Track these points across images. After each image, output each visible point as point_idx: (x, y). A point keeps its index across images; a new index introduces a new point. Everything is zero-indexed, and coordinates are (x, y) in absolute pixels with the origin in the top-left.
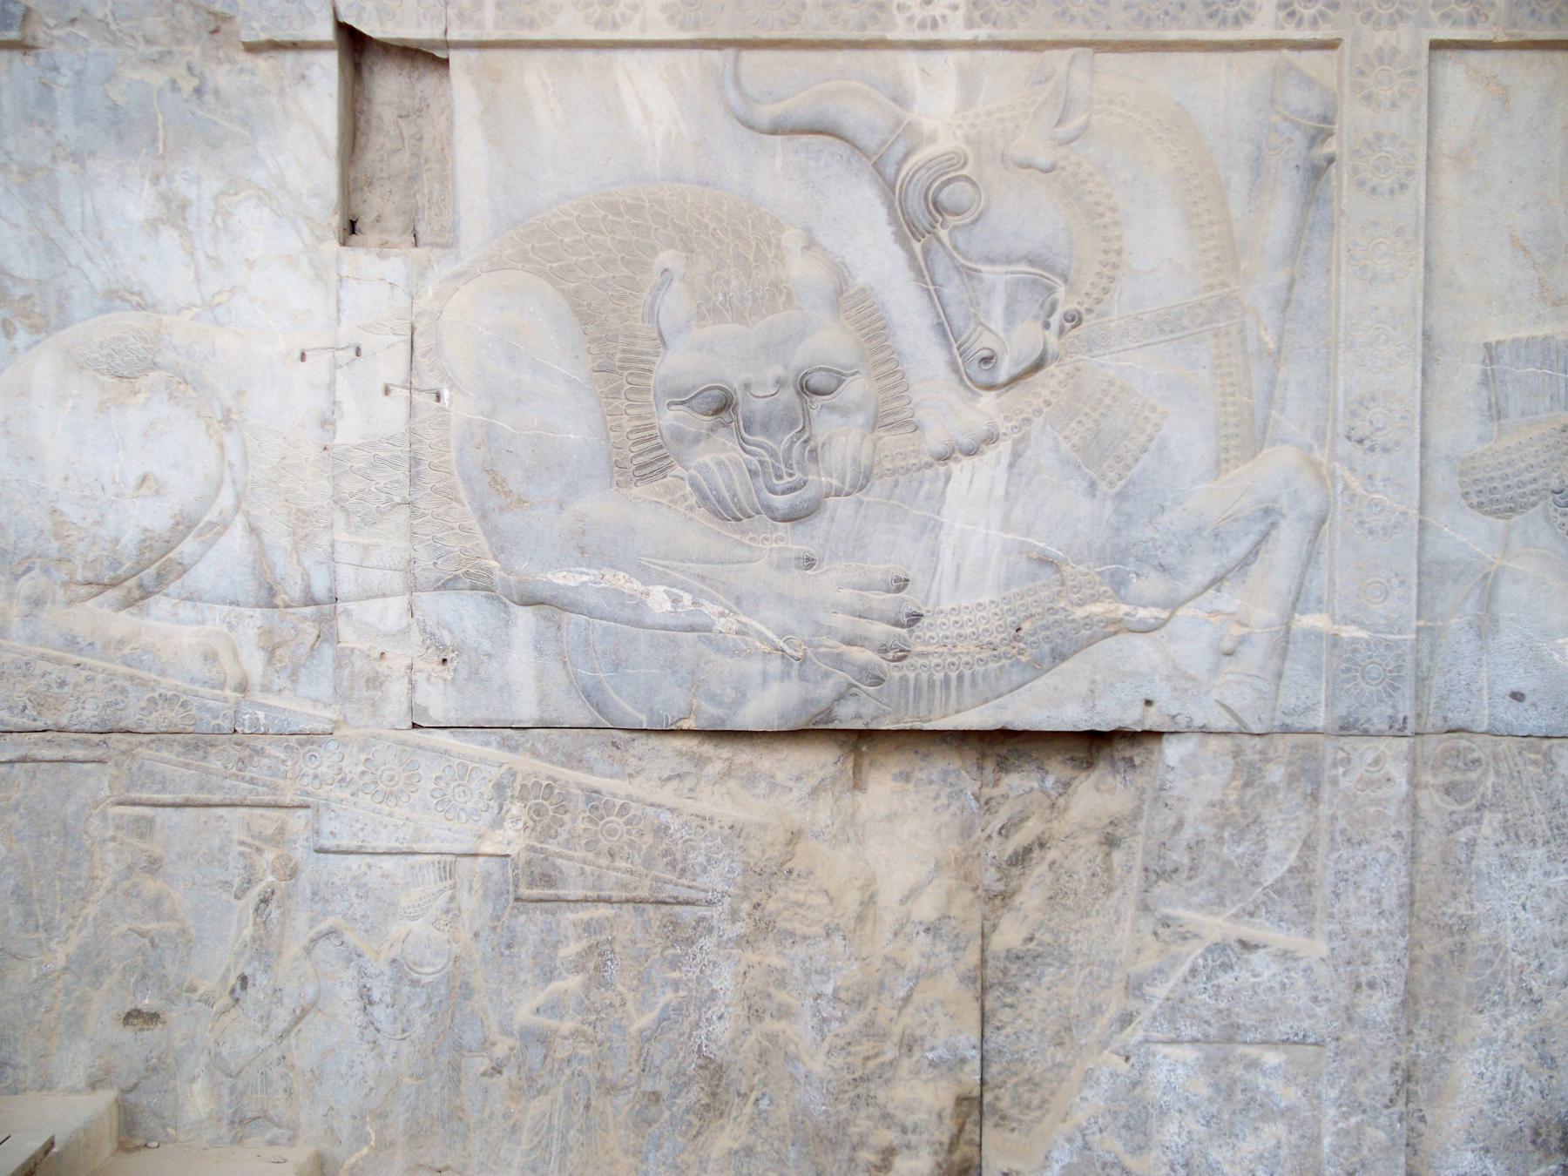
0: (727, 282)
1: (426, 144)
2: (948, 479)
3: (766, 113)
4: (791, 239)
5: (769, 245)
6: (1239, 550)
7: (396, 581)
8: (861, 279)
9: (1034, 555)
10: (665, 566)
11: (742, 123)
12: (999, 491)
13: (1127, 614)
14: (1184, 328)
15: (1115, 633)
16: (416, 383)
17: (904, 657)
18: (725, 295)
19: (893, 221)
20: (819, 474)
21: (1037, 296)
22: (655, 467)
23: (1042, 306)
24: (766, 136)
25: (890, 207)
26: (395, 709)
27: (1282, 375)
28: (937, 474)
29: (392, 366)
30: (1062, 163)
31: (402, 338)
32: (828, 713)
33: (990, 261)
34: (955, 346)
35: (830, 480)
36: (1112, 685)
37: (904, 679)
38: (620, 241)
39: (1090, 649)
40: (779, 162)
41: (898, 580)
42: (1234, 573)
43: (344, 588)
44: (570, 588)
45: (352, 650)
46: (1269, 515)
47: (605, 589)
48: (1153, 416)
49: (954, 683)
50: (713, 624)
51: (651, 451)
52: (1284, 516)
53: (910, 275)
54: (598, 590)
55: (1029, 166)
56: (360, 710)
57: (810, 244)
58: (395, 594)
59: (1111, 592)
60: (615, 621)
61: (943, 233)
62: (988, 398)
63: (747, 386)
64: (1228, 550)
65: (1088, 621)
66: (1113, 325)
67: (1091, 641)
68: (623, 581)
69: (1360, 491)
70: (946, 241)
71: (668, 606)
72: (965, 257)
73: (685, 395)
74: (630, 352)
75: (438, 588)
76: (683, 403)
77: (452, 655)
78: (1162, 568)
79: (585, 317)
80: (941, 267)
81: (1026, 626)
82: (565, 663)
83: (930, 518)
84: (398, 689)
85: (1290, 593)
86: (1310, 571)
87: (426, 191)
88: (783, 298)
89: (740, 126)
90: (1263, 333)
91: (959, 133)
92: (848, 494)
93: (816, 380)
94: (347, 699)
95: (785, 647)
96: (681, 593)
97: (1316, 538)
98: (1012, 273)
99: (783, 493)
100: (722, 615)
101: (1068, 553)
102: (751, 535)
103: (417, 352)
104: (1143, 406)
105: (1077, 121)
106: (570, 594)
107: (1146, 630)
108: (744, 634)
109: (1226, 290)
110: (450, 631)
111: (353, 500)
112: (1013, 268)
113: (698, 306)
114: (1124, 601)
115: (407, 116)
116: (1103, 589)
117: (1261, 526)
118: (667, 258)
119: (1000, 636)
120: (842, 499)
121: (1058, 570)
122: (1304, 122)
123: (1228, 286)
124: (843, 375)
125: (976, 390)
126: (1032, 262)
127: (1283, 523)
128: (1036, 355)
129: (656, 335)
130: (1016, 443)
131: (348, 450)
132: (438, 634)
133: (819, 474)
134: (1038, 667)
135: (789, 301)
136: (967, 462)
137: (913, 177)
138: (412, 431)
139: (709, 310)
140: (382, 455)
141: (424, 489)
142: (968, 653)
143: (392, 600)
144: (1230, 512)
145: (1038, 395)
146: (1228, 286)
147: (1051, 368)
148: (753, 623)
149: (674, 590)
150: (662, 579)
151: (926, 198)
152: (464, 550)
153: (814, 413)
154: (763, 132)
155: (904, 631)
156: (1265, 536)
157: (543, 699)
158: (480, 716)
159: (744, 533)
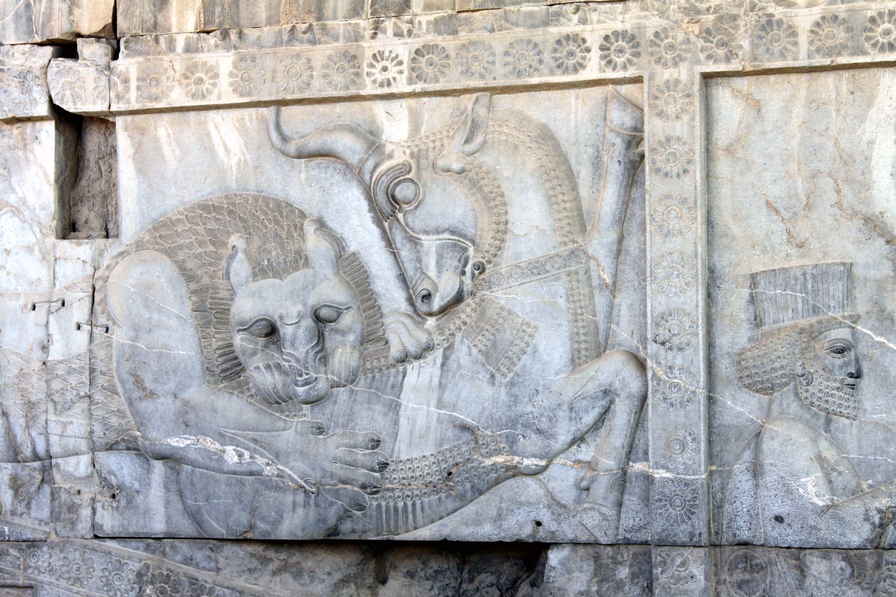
0: (270, 252)
2: (405, 374)
5: (295, 229)
6: (589, 418)
7: (83, 445)
8: (352, 247)
9: (457, 423)
12: (436, 381)
13: (518, 463)
14: (547, 272)
15: (514, 476)
16: (94, 323)
18: (268, 260)
21: (456, 254)
22: (233, 371)
23: (459, 260)
24: (295, 160)
26: (83, 527)
27: (617, 301)
28: (398, 372)
29: (79, 312)
30: (468, 167)
32: (335, 531)
33: (427, 232)
36: (512, 511)
37: (379, 506)
39: (497, 487)
40: (303, 176)
41: (373, 440)
42: (589, 434)
43: (55, 449)
44: (181, 449)
45: (60, 488)
48: (529, 330)
49: (410, 508)
50: (263, 470)
52: (618, 395)
53: (383, 244)
54: (196, 449)
55: (448, 171)
56: (64, 527)
58: (83, 453)
59: (507, 448)
60: (207, 469)
61: (400, 216)
62: (431, 322)
64: (581, 419)
65: (494, 467)
66: (503, 271)
67: (497, 482)
69: (664, 377)
70: (402, 220)
71: (236, 459)
72: (413, 231)
73: (246, 325)
75: (107, 450)
76: (245, 330)
78: (539, 432)
79: (188, 276)
80: (398, 238)
83: (394, 401)
84: (86, 512)
85: (623, 447)
86: (639, 432)
88: (303, 262)
91: (408, 151)
92: (344, 386)
94: (58, 519)
96: (243, 451)
97: (641, 409)
99: (302, 386)
100: (268, 464)
103: (96, 302)
105: (479, 139)
106: (181, 452)
107: (534, 473)
108: (282, 477)
109: (575, 245)
110: (115, 476)
111: (58, 395)
112: (441, 236)
114: (514, 453)
115: (103, 158)
116: (502, 446)
118: (236, 240)
120: (341, 389)
121: (473, 433)
122: (622, 131)
126: (453, 232)
130: (446, 349)
131: (56, 364)
132: (108, 478)
133: (326, 373)
134: (463, 500)
135: (307, 263)
136: (416, 364)
138: (90, 351)
140: (74, 366)
141: (97, 387)
142: (418, 489)
143: (81, 456)
147: (469, 301)
149: (239, 449)
150: (233, 441)
151: (387, 194)
153: (327, 334)
154: (293, 157)
155: (377, 475)
156: (607, 410)
157: (169, 518)
158: (133, 529)
159: (282, 412)
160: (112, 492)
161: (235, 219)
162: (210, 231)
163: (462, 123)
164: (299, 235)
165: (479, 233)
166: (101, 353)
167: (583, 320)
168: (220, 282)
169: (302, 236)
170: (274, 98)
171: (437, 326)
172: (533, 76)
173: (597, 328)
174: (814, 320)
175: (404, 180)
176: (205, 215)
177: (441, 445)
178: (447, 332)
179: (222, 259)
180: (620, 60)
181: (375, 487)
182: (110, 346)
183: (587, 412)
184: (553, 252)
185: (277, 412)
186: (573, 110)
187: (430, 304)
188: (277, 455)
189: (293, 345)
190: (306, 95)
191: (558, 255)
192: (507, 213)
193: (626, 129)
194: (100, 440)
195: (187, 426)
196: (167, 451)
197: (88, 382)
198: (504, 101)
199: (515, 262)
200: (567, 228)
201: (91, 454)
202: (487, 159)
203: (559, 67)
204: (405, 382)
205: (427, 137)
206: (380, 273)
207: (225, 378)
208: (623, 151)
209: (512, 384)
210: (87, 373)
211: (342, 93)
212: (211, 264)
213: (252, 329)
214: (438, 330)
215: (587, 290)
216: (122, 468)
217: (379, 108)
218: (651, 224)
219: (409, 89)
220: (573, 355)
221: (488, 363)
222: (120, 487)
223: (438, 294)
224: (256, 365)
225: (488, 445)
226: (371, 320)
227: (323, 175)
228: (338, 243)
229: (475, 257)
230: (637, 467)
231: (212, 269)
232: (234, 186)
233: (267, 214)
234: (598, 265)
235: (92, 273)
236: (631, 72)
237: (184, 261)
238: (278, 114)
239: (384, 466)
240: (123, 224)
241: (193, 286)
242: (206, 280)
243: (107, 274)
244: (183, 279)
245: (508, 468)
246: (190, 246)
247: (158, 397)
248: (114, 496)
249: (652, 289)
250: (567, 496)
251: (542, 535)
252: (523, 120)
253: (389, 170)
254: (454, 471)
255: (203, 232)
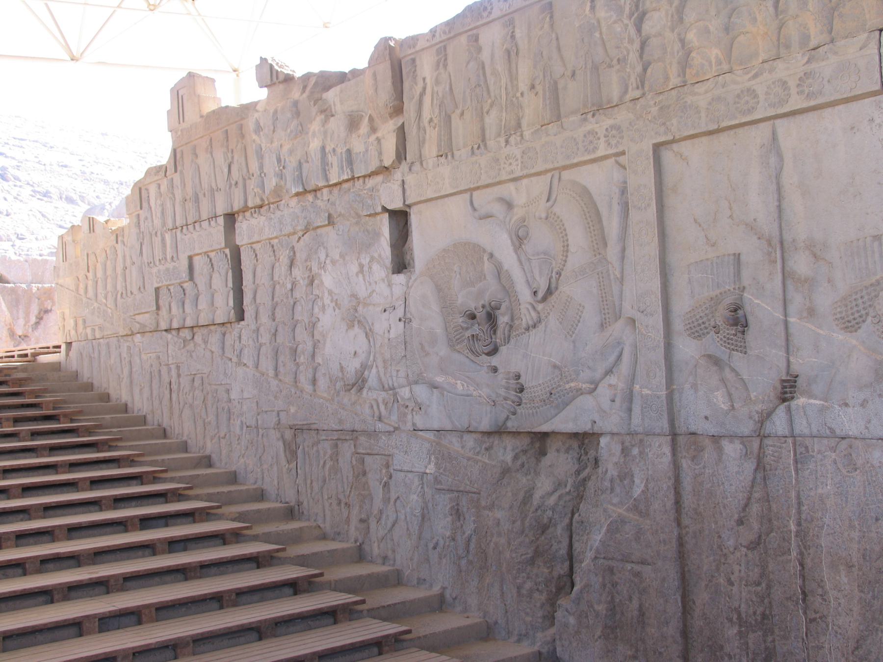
43: (395, 384)
78: (589, 368)
173: (614, 305)
174: (718, 292)
180: (613, 142)
188: (478, 385)
203: (586, 150)
238: (471, 196)
251: (596, 429)
254: (553, 392)
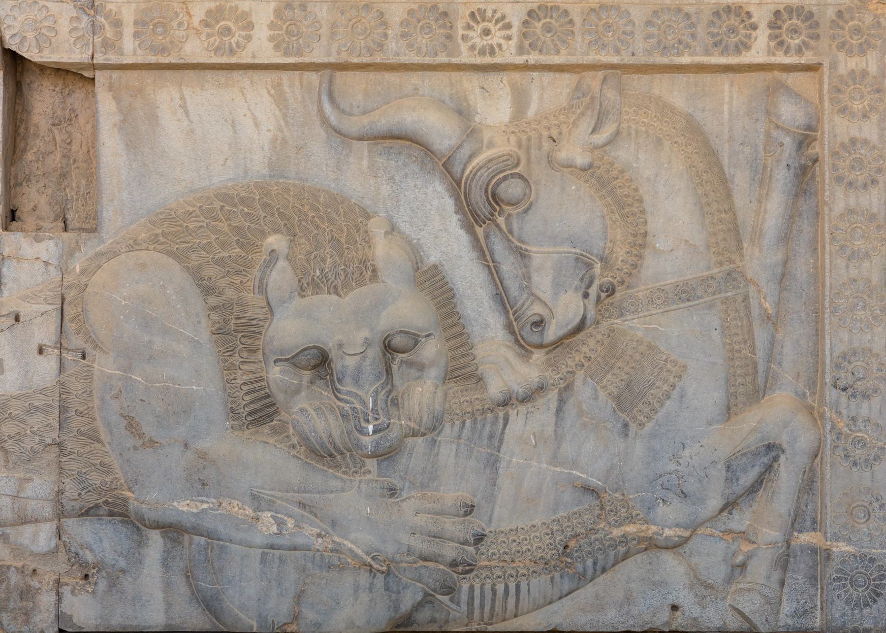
0: (324, 260)
1: (74, 148)
3: (355, 124)
4: (377, 228)
5: (358, 230)
6: (747, 479)
10: (272, 496)
11: (336, 131)
12: (550, 429)
13: (654, 533)
14: (699, 298)
16: (65, 344)
17: (471, 571)
18: (322, 271)
19: (459, 210)
20: (399, 418)
22: (263, 413)
23: (582, 279)
25: (457, 199)
27: (779, 336)
30: (597, 163)
31: (55, 307)
34: (511, 312)
35: (409, 423)
38: (235, 227)
40: (365, 163)
41: (465, 505)
42: (743, 498)
46: (772, 449)
47: (220, 514)
48: (674, 369)
51: (260, 399)
52: (783, 451)
53: (474, 255)
57: (393, 229)
61: (501, 220)
62: (538, 356)
63: (340, 346)
64: (737, 480)
66: (640, 294)
68: (237, 509)
70: (503, 226)
71: (274, 529)
74: (243, 318)
75: (79, 516)
76: (287, 360)
77: (93, 571)
78: (684, 495)
80: (499, 247)
81: (572, 544)
82: (188, 577)
83: (492, 455)
87: (74, 185)
88: (369, 273)
89: (334, 133)
90: (763, 300)
91: (513, 138)
92: (423, 435)
93: (398, 341)
95: (373, 563)
96: (286, 518)
98: (558, 253)
100: (319, 535)
101: (606, 483)
102: (343, 469)
103: (66, 318)
104: (666, 361)
108: (337, 551)
109: (732, 266)
110: (91, 550)
113: (300, 280)
115: (58, 125)
117: (765, 460)
118: (275, 241)
119: (550, 553)
120: (420, 440)
121: (598, 497)
123: (734, 263)
124: (419, 336)
125: (529, 348)
127: (782, 458)
128: (577, 320)
129: (265, 304)
132: (81, 553)
133: (399, 418)
135: (375, 276)
136: (522, 409)
137: (476, 174)
138: (61, 384)
139: (308, 284)
141: (71, 432)
144: (739, 448)
145: (580, 351)
146: (734, 263)
148: (346, 542)
149: (279, 515)
150: (271, 505)
151: (486, 191)
152: (103, 483)
153: (395, 367)
155: (471, 549)
156: (769, 468)
160: (85, 572)
161: (273, 215)
162: (238, 230)
163: (587, 108)
164: (364, 240)
165: (608, 245)
166: (76, 387)
167: (741, 358)
168: (252, 298)
169: (368, 242)
170: (332, 60)
171: (548, 361)
172: (683, 55)
173: (756, 368)
175: (513, 175)
176: (227, 208)
177: (555, 511)
178: (565, 370)
179: (254, 267)
181: (469, 565)
182: (89, 377)
183: (745, 470)
184: (706, 273)
185: (330, 467)
186: (727, 99)
187: (542, 333)
189: (357, 382)
190: (378, 58)
191: (712, 278)
192: (646, 222)
193: (798, 127)
194: (73, 503)
195: (204, 485)
196: (172, 518)
197: (57, 425)
198: (638, 83)
199: (657, 285)
200: (723, 245)
201: (56, 522)
202: (623, 154)
204: (507, 431)
205: (539, 122)
206: (469, 291)
207: (253, 422)
208: (794, 154)
209: (653, 435)
210: (56, 412)
211: (428, 60)
212: (237, 273)
213: (296, 360)
214: (550, 366)
215: (745, 322)
216: (101, 541)
217: (470, 83)
218: (831, 243)
219: (519, 60)
220: (729, 401)
221: (620, 409)
222: (99, 566)
223: (554, 321)
224: (300, 406)
225: (617, 511)
226: (458, 352)
227: (393, 163)
228: (415, 251)
229: (602, 275)
230: (805, 538)
231: (238, 279)
232: (265, 171)
233: (318, 210)
234: (759, 291)
235: (59, 278)
236: (808, 58)
237: (199, 267)
238: (331, 82)
239: (479, 539)
240: (105, 214)
241: (213, 300)
242: (230, 293)
243: (84, 279)
244: (198, 291)
245: (641, 540)
246: (208, 247)
247: (162, 446)
248: (86, 577)
249: (831, 323)
250: (718, 573)
252: (664, 109)
253: (490, 161)
255: (226, 229)
